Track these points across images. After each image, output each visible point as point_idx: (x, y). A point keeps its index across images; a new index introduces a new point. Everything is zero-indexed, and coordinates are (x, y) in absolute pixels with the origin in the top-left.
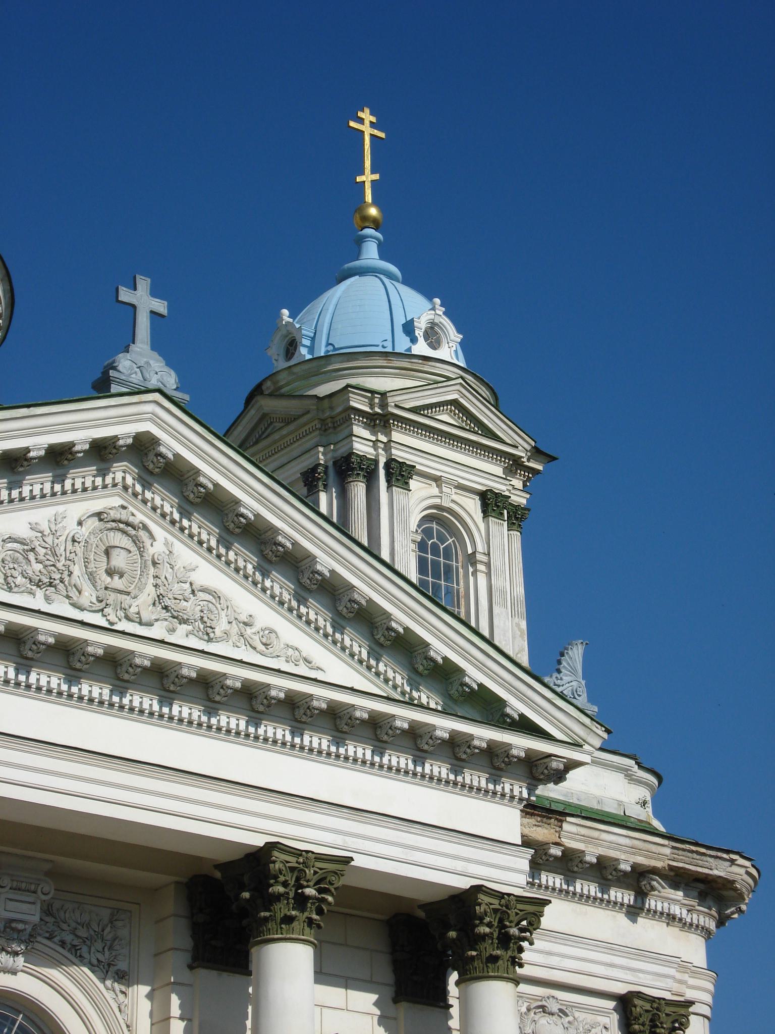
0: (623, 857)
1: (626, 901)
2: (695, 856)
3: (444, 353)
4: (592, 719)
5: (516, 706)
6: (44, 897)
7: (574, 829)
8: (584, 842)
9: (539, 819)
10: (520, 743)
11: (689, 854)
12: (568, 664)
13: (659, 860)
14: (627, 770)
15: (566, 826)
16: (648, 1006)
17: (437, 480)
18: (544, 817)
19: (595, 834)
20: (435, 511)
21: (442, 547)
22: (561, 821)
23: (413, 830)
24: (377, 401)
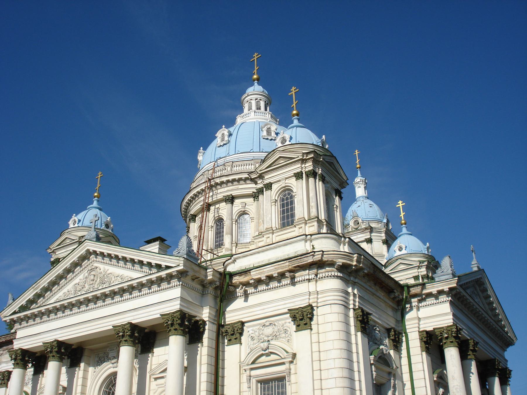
0: (273, 273)
1: (289, 282)
2: (299, 260)
3: (288, 143)
4: (179, 257)
5: (164, 264)
6: (116, 350)
7: (255, 273)
8: (259, 275)
9: (244, 275)
10: (163, 274)
11: (296, 261)
12: (181, 244)
13: (286, 267)
14: (304, 239)
15: (252, 273)
16: (297, 311)
17: (279, 181)
18: (245, 274)
19: (262, 271)
20: (283, 189)
21: (289, 197)
22: (250, 273)
23: (149, 307)
24: (256, 173)
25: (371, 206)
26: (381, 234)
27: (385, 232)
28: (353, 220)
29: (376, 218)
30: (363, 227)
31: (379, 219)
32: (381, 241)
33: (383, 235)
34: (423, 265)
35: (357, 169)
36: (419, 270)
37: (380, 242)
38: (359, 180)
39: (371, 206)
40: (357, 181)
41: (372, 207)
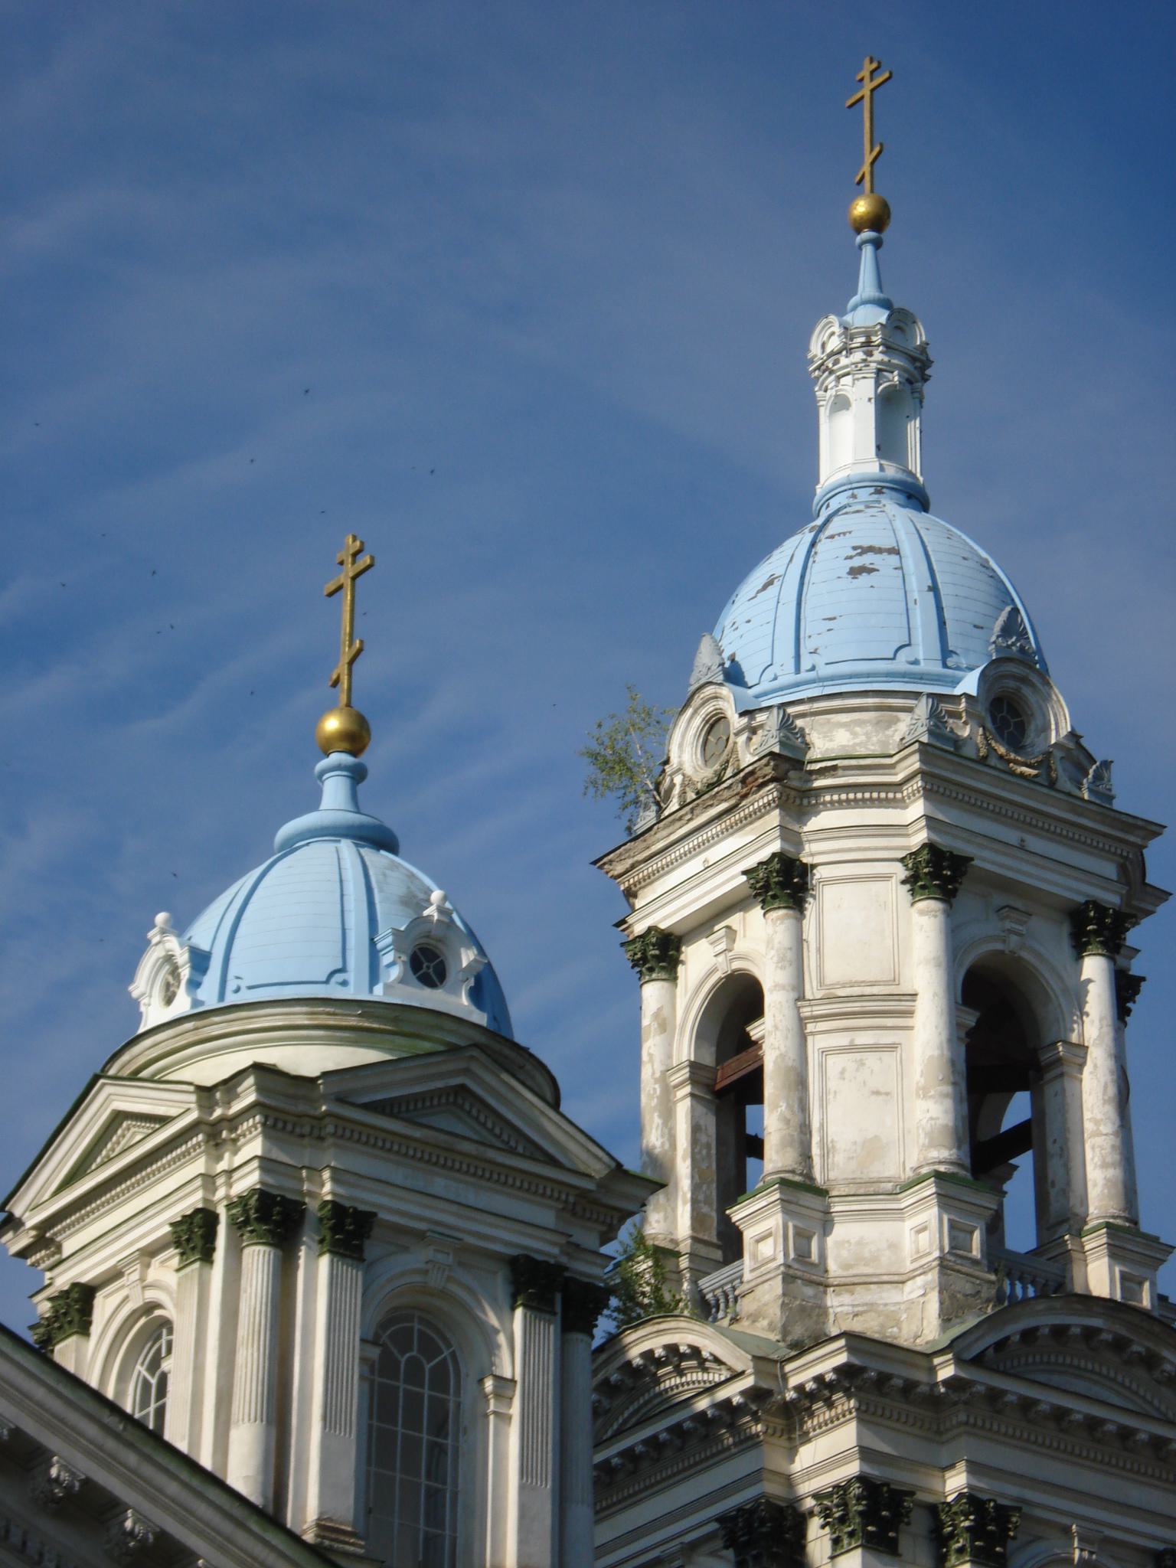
25: (867, 560)
26: (900, 804)
27: (918, 783)
28: (698, 721)
29: (901, 664)
30: (747, 758)
31: (921, 678)
32: (899, 865)
33: (917, 809)
34: (237, 1106)
35: (859, 231)
36: (227, 1155)
37: (886, 877)
38: (834, 344)
39: (867, 560)
40: (828, 350)
41: (870, 571)
